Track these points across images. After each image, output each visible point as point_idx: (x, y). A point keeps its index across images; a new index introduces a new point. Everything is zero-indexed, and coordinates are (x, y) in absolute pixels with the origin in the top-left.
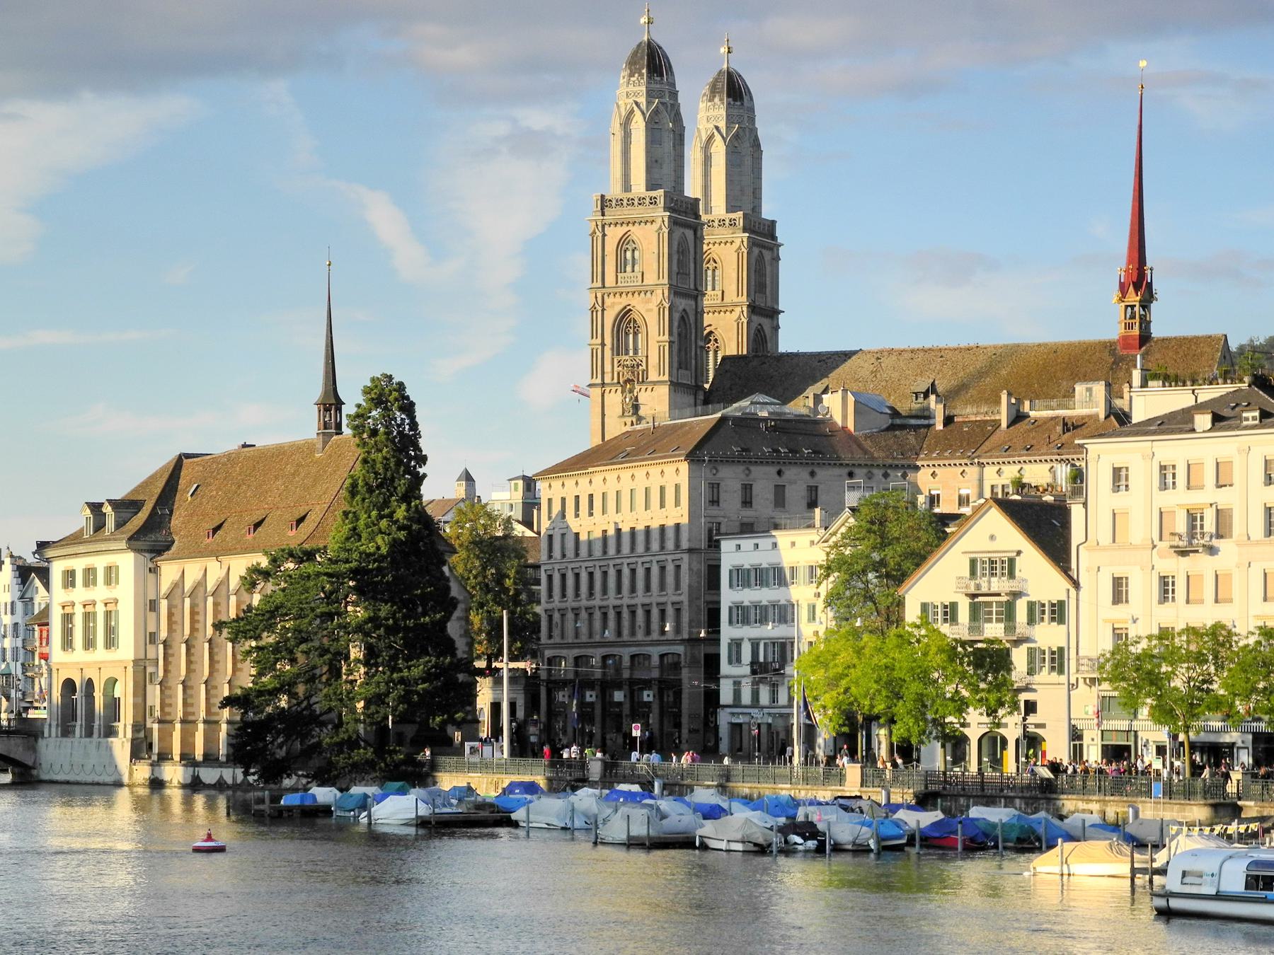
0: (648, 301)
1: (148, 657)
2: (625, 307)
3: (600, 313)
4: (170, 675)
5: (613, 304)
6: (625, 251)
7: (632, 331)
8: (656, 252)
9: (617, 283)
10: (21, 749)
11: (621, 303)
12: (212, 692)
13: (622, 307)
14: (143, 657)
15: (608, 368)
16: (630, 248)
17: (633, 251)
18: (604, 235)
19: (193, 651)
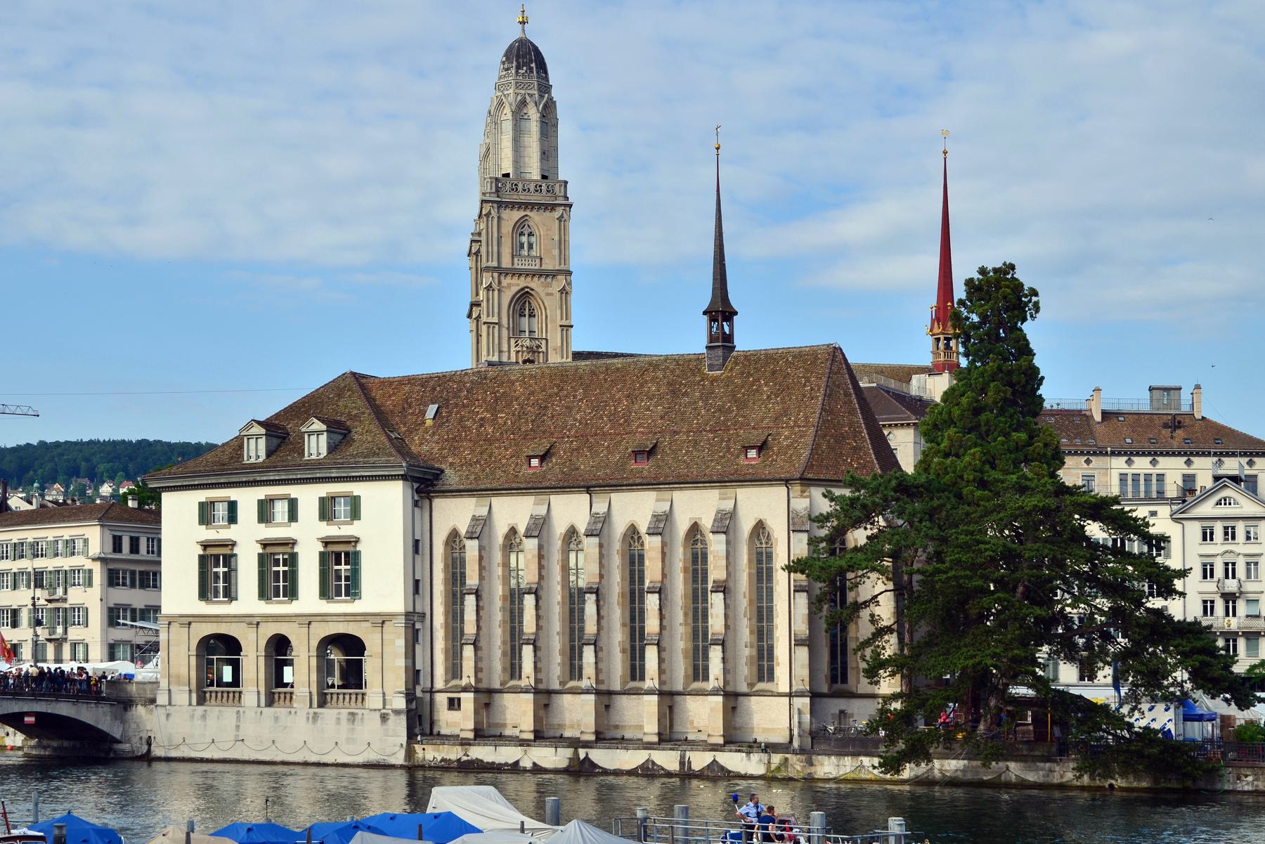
0: (549, 285)
1: (417, 611)
2: (523, 289)
3: (496, 292)
4: (482, 633)
5: (509, 286)
6: (520, 235)
7: (527, 312)
8: (557, 238)
9: (513, 264)
10: (108, 718)
11: (518, 285)
12: (600, 654)
13: (515, 289)
14: (411, 610)
15: (505, 348)
16: (526, 233)
17: (529, 235)
18: (499, 218)
19: (541, 603)
